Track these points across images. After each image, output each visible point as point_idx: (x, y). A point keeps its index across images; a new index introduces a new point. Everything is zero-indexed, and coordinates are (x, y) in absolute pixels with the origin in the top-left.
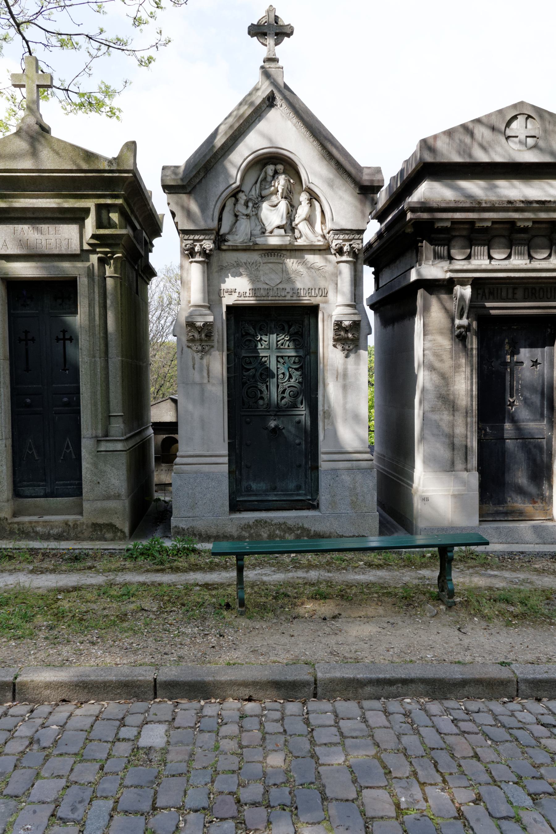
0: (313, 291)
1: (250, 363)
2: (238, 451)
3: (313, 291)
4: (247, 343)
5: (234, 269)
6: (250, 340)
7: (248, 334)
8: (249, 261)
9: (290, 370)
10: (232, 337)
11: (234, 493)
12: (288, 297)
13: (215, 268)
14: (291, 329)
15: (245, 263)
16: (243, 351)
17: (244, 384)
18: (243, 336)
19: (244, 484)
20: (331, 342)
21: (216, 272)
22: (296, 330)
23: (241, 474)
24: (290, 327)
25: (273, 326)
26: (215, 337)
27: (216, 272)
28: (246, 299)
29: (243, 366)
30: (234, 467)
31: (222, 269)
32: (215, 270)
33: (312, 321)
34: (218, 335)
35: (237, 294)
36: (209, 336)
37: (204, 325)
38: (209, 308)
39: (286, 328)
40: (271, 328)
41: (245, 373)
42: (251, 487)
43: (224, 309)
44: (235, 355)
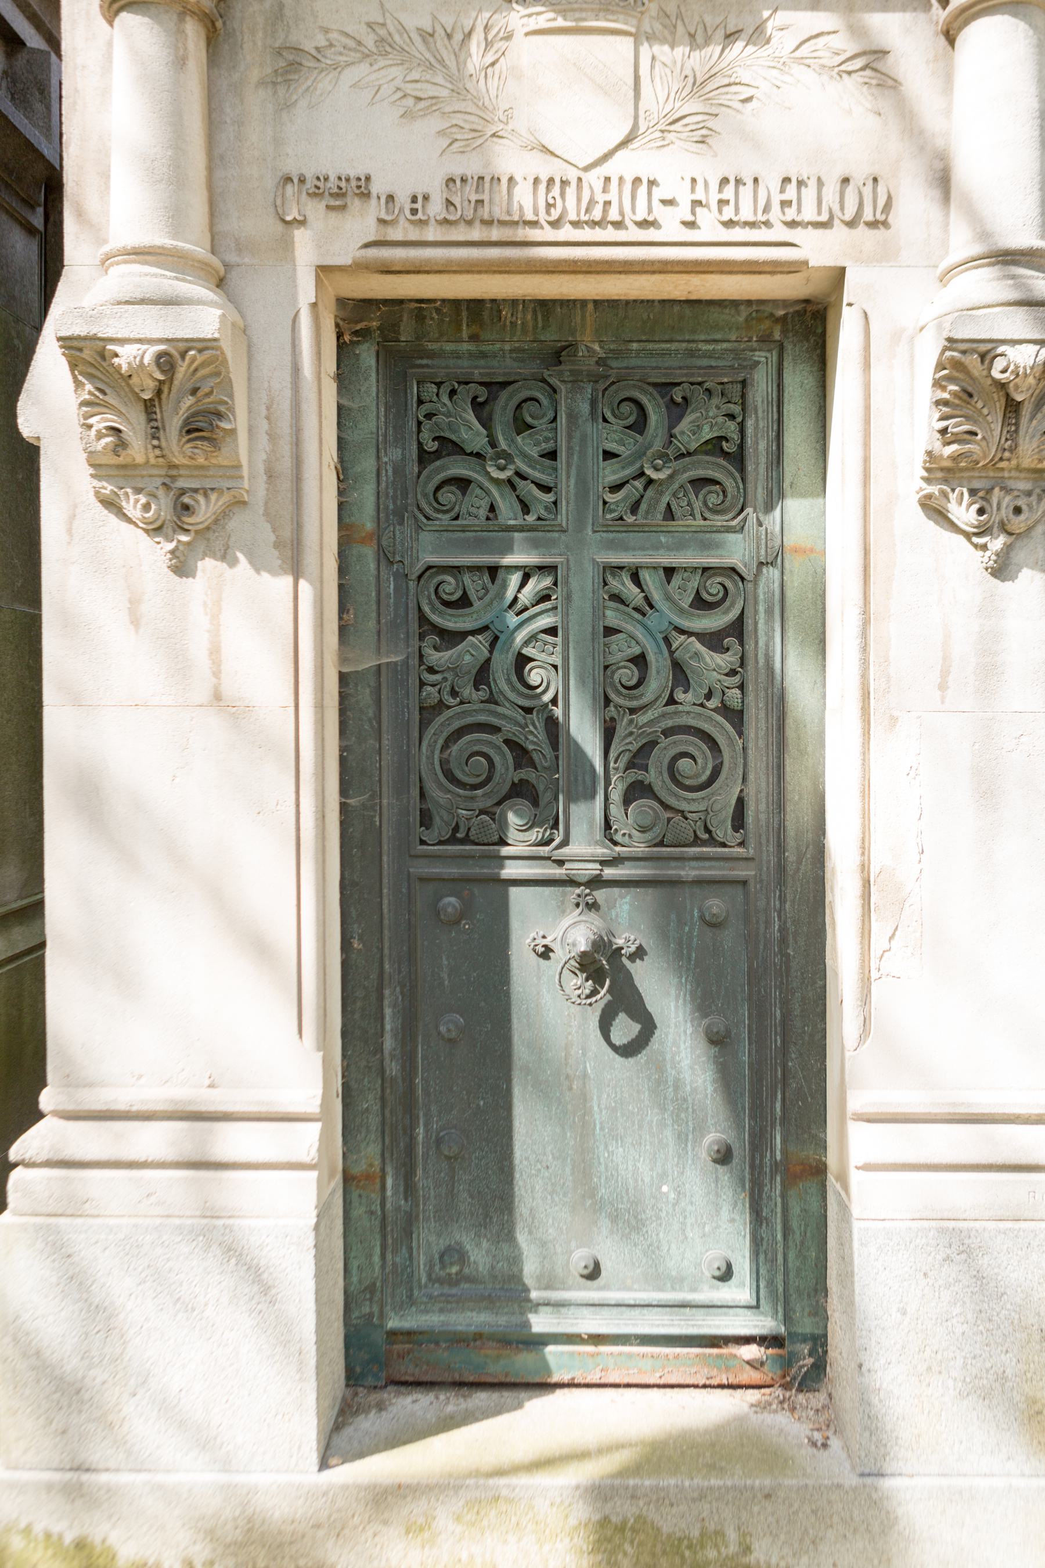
0: (809, 194)
1: (464, 602)
2: (393, 1068)
3: (809, 194)
4: (448, 496)
5: (362, 70)
6: (463, 484)
7: (449, 447)
8: (448, 20)
9: (678, 640)
10: (367, 464)
11: (371, 1289)
12: (671, 228)
13: (253, 59)
14: (685, 425)
15: (426, 36)
16: (425, 537)
17: (428, 712)
18: (424, 458)
19: (429, 1240)
20: (910, 482)
21: (262, 83)
22: (707, 434)
23: (409, 1188)
24: (677, 409)
25: (585, 408)
26: (247, 445)
27: (262, 83)
28: (432, 234)
29: (423, 618)
30: (371, 1151)
31: (294, 66)
32: (255, 75)
33: (797, 381)
34: (272, 437)
35: (374, 210)
36: (204, 426)
37: (166, 362)
38: (221, 283)
39: (655, 417)
40: (572, 417)
41: (435, 657)
42: (462, 1257)
43: (306, 291)
44: (385, 557)
